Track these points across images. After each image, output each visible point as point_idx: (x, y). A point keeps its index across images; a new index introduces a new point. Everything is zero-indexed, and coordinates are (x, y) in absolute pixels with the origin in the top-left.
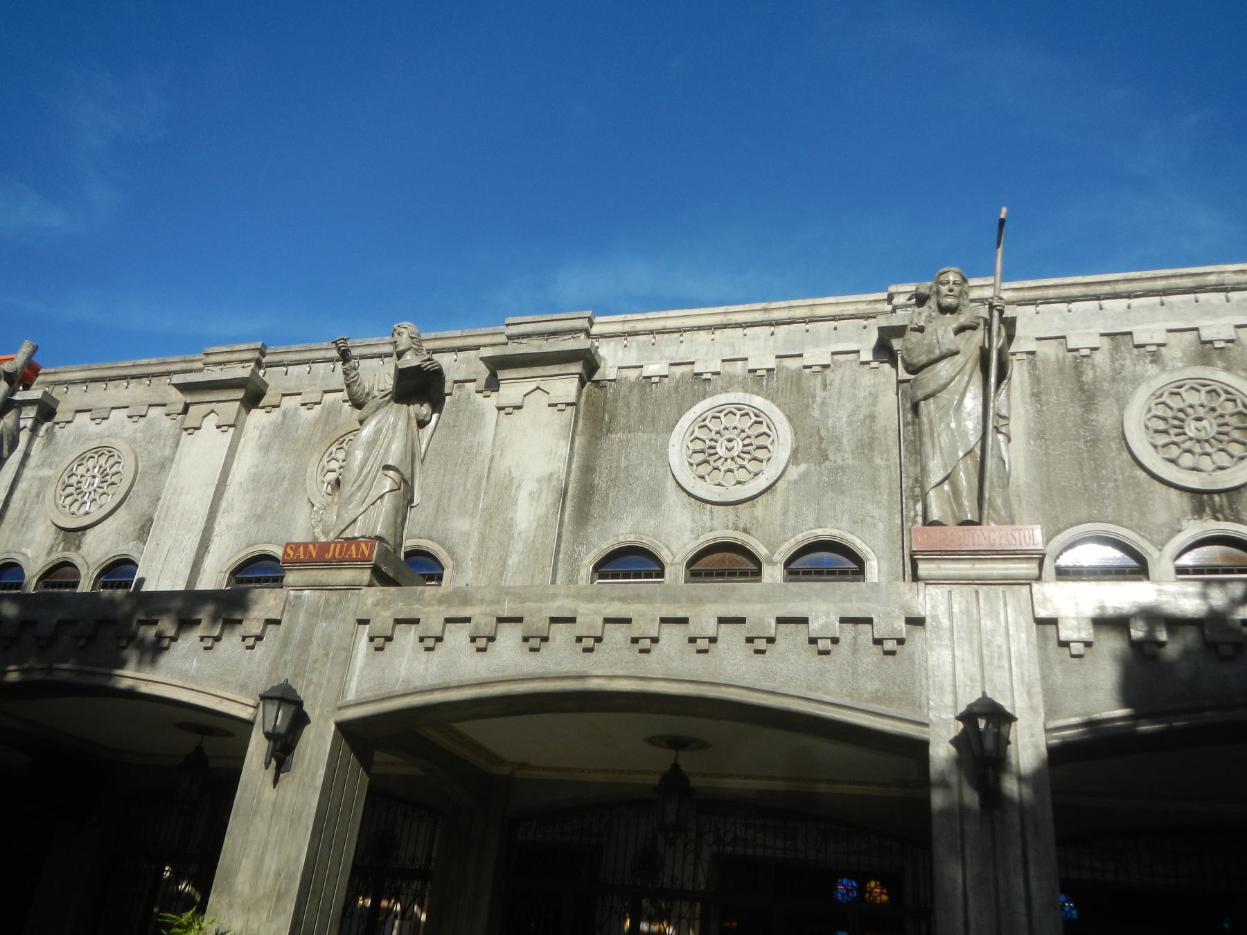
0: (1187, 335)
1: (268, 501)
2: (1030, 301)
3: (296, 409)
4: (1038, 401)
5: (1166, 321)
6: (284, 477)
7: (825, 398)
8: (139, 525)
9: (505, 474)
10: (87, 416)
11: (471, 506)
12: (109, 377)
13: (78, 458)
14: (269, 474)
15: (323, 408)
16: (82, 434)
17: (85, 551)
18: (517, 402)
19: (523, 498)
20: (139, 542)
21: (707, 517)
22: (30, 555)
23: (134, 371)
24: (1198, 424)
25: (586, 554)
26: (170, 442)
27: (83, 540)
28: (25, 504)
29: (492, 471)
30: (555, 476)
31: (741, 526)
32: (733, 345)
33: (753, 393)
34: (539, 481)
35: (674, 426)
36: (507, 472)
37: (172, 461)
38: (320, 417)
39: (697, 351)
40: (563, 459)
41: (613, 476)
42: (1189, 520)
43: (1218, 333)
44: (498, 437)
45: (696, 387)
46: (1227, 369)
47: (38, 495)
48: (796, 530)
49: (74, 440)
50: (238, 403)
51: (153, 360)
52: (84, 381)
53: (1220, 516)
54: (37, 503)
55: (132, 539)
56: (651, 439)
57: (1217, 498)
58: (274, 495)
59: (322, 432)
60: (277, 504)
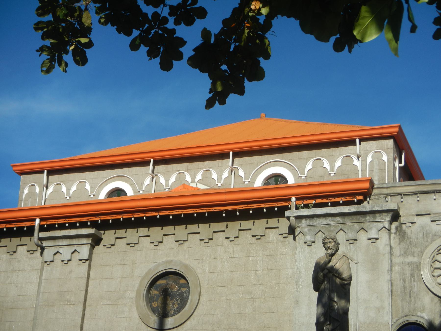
12: (436, 191)
13: (436, 249)
28: (404, 281)
47: (412, 275)
49: (423, 235)
52: (416, 193)
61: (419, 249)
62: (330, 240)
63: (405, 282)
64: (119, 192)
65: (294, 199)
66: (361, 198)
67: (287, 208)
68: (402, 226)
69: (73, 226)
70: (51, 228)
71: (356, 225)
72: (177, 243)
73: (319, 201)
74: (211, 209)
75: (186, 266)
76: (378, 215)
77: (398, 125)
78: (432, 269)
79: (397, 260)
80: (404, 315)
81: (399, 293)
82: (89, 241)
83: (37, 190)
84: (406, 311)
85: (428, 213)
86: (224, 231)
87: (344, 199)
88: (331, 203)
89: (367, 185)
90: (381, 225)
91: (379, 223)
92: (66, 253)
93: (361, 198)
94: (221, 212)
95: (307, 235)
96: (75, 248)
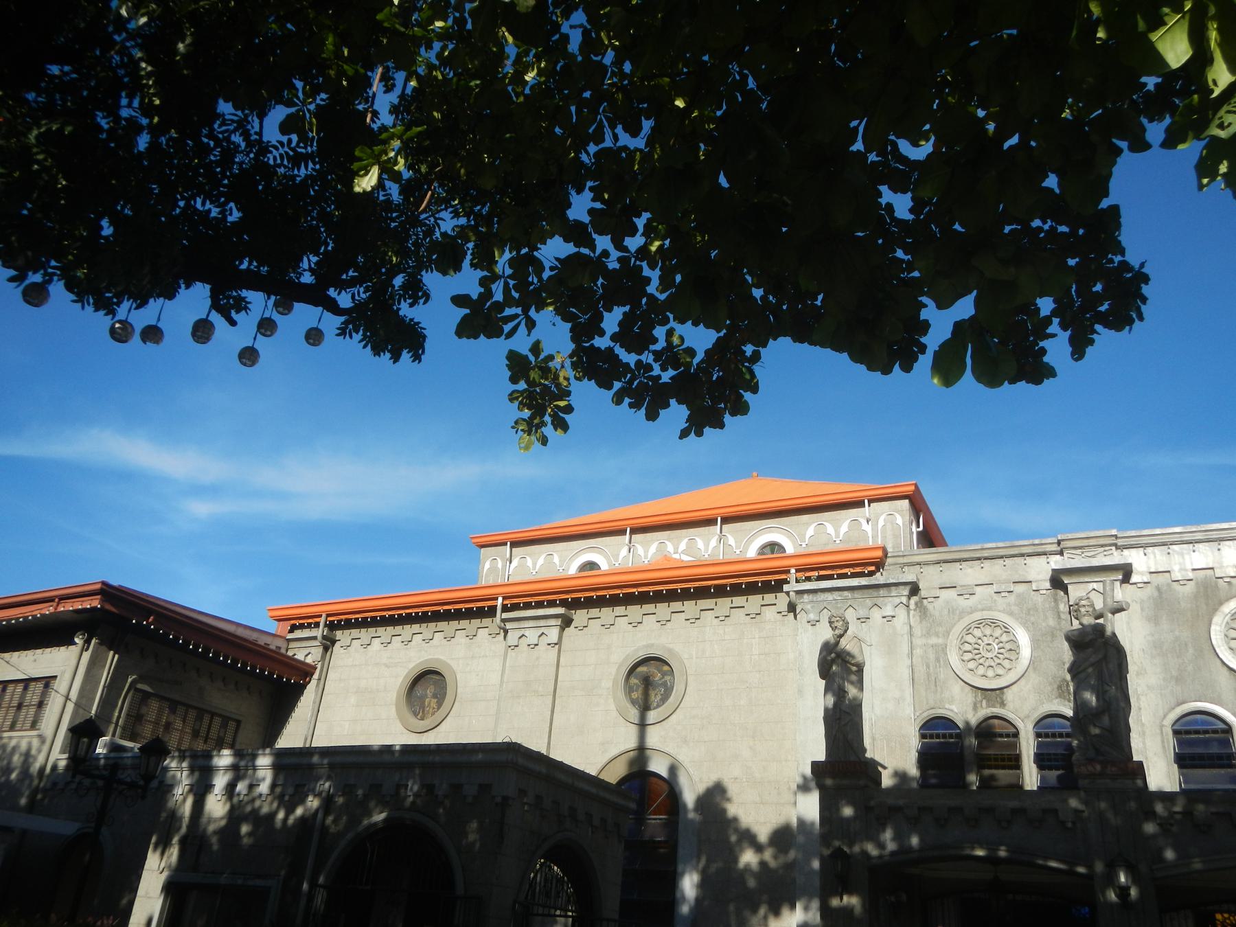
1: (1180, 665)
3: (1168, 585)
6: (1186, 645)
8: (1056, 686)
10: (951, 594)
14: (1169, 641)
15: (1197, 583)
16: (955, 608)
17: (1012, 707)
20: (1063, 700)
22: (956, 710)
23: (986, 554)
26: (1049, 614)
27: (1004, 697)
28: (928, 667)
38: (1197, 592)
47: (938, 660)
51: (1001, 544)
54: (940, 667)
55: (1053, 697)
58: (1183, 660)
59: (1207, 604)
60: (1190, 668)
61: (944, 629)
62: (838, 618)
63: (929, 668)
64: (591, 566)
65: (793, 571)
66: (873, 568)
67: (786, 582)
68: (922, 602)
69: (540, 605)
70: (515, 607)
71: (868, 601)
72: (659, 624)
73: (823, 573)
74: (697, 584)
75: (670, 651)
76: (893, 588)
77: (914, 482)
78: (961, 652)
79: (918, 641)
80: (928, 708)
81: (922, 681)
82: (559, 622)
83: (500, 565)
84: (932, 703)
85: (954, 585)
86: (713, 609)
87: (852, 571)
88: (837, 574)
89: (879, 553)
90: (897, 600)
91: (895, 598)
92: (532, 635)
93: (873, 568)
94: (709, 587)
95: (810, 613)
96: (542, 630)
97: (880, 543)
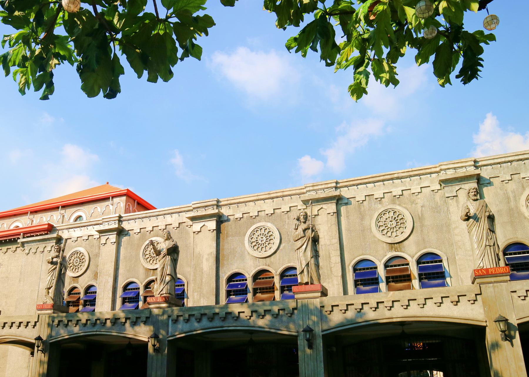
0: (389, 194)
2: (345, 186)
4: (348, 219)
5: (383, 190)
7: (288, 222)
9: (198, 253)
11: (190, 263)
18: (199, 230)
19: (204, 260)
21: (258, 263)
24: (391, 223)
25: (225, 276)
29: (194, 253)
30: (213, 253)
31: (267, 264)
32: (260, 206)
33: (267, 222)
34: (208, 255)
35: (246, 234)
36: (199, 253)
37: (99, 253)
39: (250, 209)
40: (214, 247)
41: (230, 251)
42: (388, 252)
43: (397, 193)
44: (194, 242)
45: (251, 221)
46: (399, 205)
48: (283, 264)
50: (116, 235)
53: (397, 250)
56: (239, 239)
57: (396, 245)
65: (22, 234)
67: (19, 238)
97: (46, 223)
